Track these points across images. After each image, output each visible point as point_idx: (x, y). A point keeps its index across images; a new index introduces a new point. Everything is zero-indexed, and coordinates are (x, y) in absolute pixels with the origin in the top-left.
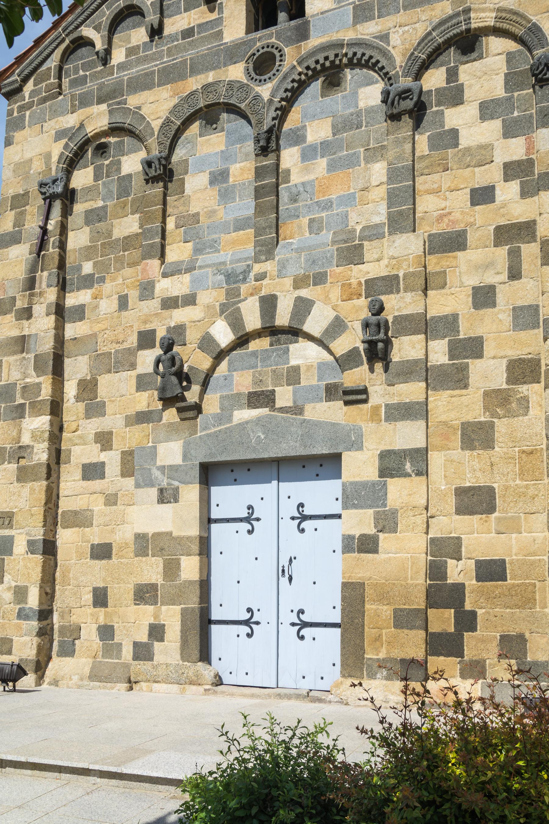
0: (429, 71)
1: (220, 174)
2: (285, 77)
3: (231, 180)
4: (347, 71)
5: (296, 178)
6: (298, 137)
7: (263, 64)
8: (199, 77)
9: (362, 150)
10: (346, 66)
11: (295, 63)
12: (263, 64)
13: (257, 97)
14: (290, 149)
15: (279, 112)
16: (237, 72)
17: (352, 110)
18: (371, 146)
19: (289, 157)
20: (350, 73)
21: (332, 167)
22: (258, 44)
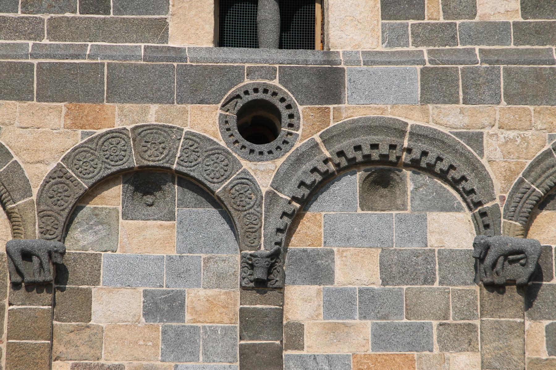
0: (544, 212)
1: (165, 301)
2: (299, 159)
3: (188, 317)
4: (408, 173)
5: (314, 344)
6: (318, 270)
7: (259, 124)
8: (127, 105)
9: (435, 323)
10: (406, 166)
11: (317, 137)
12: (259, 124)
13: (247, 181)
14: (303, 287)
15: (286, 220)
16: (206, 121)
17: (415, 247)
18: (451, 321)
19: (301, 302)
20: (412, 180)
21: (381, 338)
22: (247, 81)
